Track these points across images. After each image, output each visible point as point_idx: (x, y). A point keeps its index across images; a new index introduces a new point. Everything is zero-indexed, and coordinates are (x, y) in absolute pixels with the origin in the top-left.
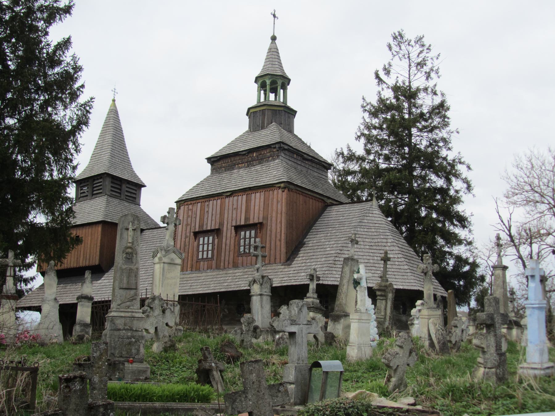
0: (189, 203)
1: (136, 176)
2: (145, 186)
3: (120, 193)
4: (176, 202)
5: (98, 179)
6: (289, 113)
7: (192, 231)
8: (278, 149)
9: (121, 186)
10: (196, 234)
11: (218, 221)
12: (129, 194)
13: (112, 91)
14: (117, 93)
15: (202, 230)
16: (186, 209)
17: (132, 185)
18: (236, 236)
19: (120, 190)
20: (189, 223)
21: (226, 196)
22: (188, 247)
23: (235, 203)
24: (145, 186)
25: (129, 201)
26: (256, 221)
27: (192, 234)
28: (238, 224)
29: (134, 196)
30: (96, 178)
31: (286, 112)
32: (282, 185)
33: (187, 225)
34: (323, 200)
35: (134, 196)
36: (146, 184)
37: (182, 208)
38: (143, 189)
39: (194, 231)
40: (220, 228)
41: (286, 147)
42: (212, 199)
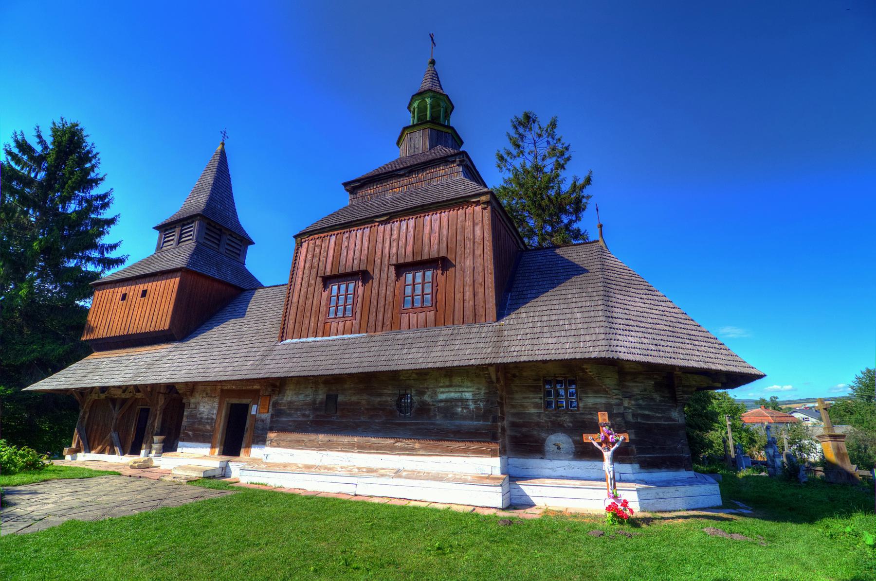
0: (316, 236)
1: (242, 229)
2: (252, 243)
3: (218, 245)
4: (296, 237)
5: (188, 224)
6: (455, 140)
7: (319, 275)
8: (459, 163)
9: (220, 236)
10: (327, 280)
11: (364, 257)
12: (231, 249)
13: (221, 133)
14: (228, 138)
15: (335, 273)
16: (311, 245)
17: (236, 238)
18: (397, 280)
19: (219, 241)
20: (316, 264)
21: (379, 222)
22: (311, 300)
23: (395, 232)
24: (253, 243)
25: (230, 257)
26: (435, 255)
27: (319, 280)
28: (401, 261)
29: (238, 252)
30: (185, 222)
31: (454, 138)
32: (484, 198)
33: (311, 267)
34: (518, 243)
35: (238, 252)
36: (254, 241)
37: (305, 245)
38: (250, 247)
39: (322, 275)
40: (369, 270)
41: (469, 163)
42: (356, 228)
